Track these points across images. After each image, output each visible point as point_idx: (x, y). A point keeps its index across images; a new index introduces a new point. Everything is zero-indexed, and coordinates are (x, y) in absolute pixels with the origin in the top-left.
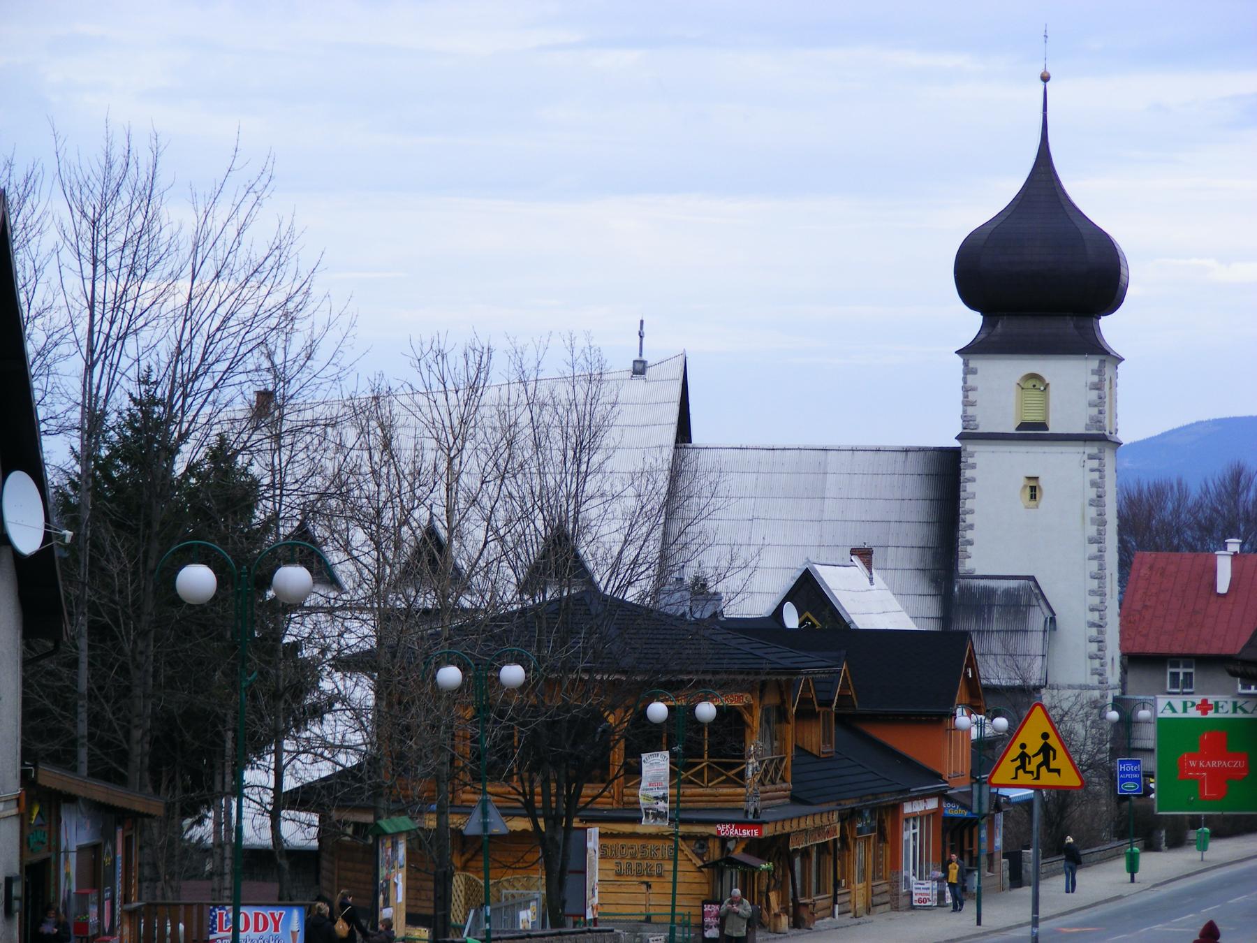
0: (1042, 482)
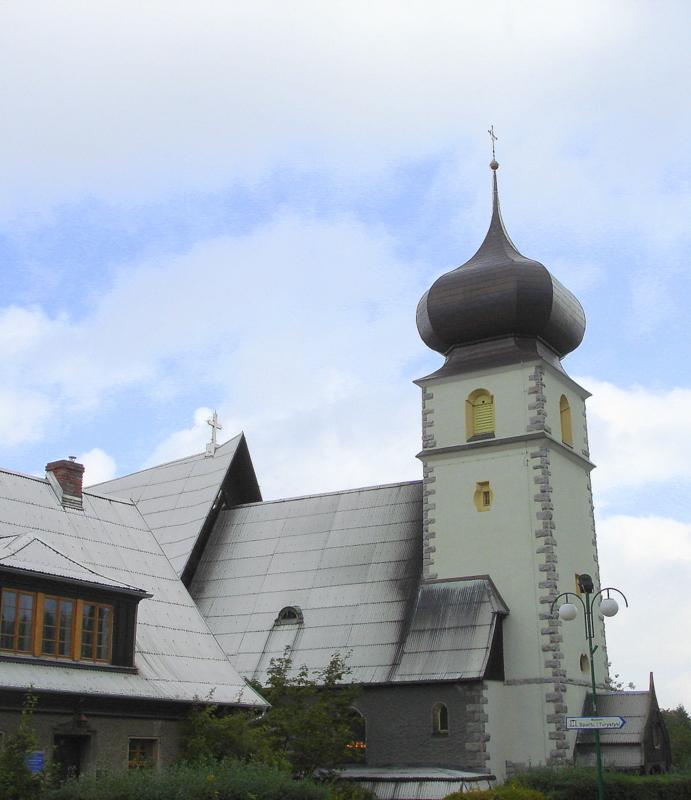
0: (492, 487)
